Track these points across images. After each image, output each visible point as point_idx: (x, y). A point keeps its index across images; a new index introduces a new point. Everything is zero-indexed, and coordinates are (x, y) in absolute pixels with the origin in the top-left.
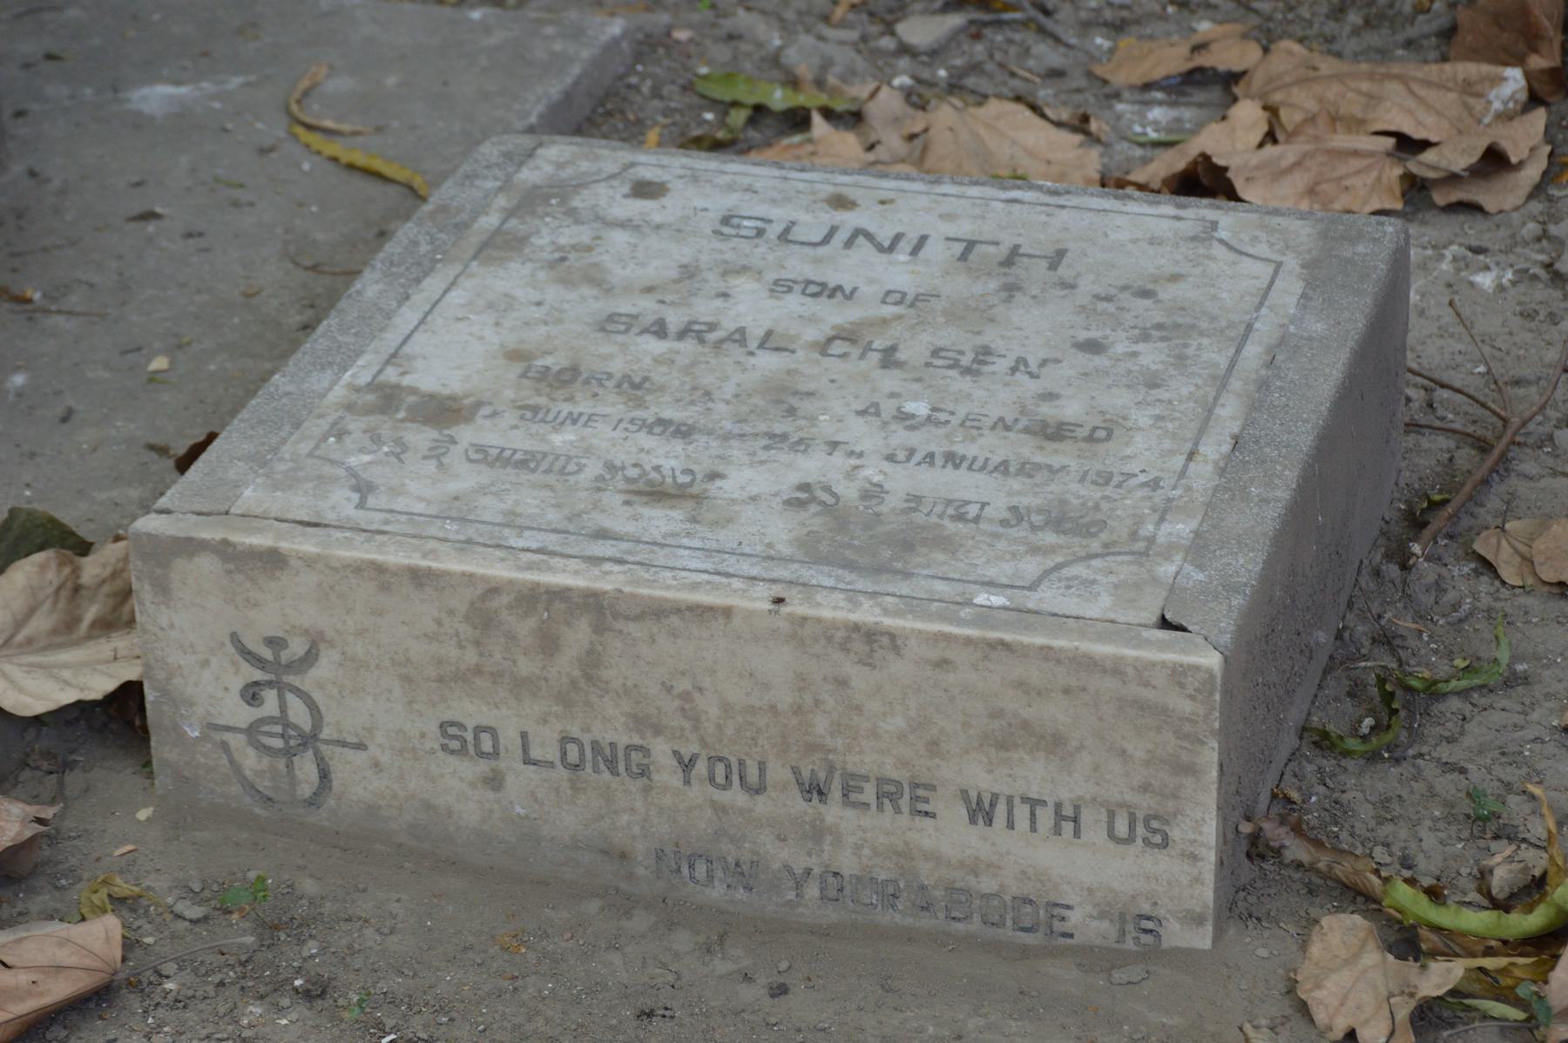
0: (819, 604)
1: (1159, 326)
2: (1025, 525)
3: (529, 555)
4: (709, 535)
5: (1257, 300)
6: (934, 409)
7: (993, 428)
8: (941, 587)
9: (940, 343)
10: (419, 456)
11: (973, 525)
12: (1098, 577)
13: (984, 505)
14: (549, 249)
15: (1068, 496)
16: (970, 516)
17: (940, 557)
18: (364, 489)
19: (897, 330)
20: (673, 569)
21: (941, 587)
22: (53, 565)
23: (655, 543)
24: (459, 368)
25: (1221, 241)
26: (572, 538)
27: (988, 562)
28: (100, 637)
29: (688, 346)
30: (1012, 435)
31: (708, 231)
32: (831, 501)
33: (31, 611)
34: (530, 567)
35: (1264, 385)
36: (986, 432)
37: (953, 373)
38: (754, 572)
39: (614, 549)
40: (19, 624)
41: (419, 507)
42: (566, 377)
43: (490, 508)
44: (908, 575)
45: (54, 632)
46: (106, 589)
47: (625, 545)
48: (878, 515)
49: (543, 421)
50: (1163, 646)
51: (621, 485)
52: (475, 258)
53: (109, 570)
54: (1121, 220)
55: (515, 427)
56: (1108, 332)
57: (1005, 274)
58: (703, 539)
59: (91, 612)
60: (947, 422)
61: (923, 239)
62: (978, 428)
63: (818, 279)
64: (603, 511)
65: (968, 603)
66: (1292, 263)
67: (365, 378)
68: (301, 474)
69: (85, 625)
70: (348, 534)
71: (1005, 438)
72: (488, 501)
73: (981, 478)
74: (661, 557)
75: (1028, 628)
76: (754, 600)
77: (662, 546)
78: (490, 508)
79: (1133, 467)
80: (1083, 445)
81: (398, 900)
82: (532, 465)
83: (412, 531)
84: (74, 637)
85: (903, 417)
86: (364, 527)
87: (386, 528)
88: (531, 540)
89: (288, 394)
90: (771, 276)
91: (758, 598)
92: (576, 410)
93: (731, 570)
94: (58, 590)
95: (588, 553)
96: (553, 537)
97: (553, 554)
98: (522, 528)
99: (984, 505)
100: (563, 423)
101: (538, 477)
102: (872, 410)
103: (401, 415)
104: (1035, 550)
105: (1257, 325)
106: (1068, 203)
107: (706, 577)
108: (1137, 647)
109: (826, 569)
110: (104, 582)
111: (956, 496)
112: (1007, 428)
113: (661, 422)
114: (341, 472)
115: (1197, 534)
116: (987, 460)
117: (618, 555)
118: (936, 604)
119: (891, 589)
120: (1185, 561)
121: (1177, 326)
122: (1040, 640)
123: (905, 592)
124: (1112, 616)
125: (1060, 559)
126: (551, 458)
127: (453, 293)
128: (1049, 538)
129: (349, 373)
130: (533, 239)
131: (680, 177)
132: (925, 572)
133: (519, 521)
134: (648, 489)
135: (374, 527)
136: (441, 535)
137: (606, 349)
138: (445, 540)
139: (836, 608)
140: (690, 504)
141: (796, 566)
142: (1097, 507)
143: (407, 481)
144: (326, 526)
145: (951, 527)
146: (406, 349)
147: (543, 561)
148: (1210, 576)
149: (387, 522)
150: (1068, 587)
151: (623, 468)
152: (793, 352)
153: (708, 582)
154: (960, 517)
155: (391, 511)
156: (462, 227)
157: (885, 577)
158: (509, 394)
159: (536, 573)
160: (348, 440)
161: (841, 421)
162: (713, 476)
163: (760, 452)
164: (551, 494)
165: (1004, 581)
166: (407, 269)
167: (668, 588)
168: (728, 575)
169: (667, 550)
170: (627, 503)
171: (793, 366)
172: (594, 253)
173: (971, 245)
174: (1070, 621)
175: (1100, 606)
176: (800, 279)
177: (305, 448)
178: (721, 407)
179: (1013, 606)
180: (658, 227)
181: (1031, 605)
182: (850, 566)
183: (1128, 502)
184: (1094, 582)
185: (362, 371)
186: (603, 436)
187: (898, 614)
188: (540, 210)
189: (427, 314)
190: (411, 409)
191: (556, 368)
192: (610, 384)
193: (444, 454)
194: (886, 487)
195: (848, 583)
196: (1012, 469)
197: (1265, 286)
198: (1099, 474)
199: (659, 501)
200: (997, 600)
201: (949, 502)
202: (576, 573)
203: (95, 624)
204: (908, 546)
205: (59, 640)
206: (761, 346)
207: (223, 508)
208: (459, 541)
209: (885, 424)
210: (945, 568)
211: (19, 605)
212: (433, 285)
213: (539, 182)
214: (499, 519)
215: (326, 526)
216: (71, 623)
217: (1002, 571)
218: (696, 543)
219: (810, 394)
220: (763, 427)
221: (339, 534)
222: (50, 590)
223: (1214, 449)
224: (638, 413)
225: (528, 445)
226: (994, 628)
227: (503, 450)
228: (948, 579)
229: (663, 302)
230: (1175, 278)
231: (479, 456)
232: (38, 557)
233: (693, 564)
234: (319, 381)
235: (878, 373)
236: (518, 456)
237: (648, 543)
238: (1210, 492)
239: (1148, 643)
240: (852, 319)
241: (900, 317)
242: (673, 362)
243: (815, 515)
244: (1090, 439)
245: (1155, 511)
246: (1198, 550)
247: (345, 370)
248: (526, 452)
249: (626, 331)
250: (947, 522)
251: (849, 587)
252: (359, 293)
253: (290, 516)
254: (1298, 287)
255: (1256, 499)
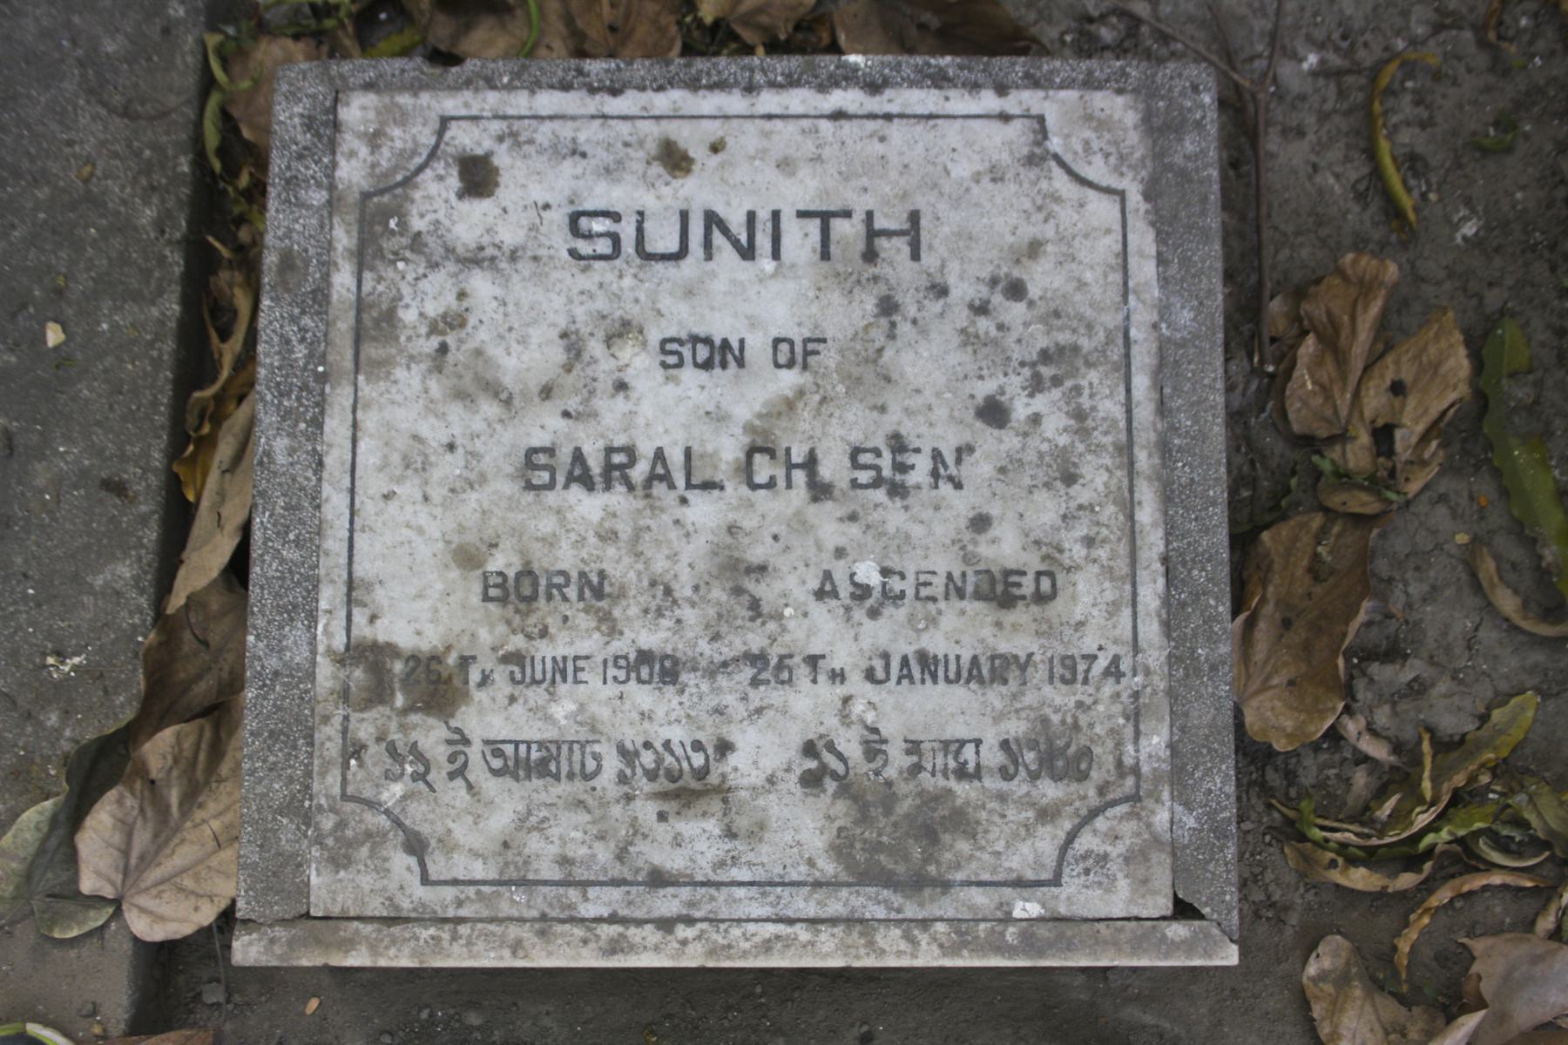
0: (883, 951)
1: (1045, 356)
2: (1023, 773)
3: (605, 926)
4: (751, 856)
5: (1116, 277)
6: (886, 572)
7: (947, 597)
8: (981, 899)
9: (856, 437)
10: (444, 773)
11: (976, 783)
12: (1109, 849)
13: (978, 743)
14: (423, 330)
15: (1047, 711)
16: (971, 767)
17: (964, 846)
18: (416, 846)
19: (805, 420)
20: (739, 921)
21: (981, 899)
22: (127, 794)
23: (707, 884)
24: (420, 596)
25: (1056, 157)
26: (634, 890)
27: (1008, 846)
28: (191, 808)
29: (618, 498)
30: (965, 604)
31: (565, 254)
32: (841, 769)
33: (129, 835)
34: (614, 947)
35: (1164, 448)
36: (942, 605)
37: (880, 495)
38: (811, 911)
39: (676, 902)
40: (126, 853)
41: (479, 871)
42: (527, 591)
43: (542, 855)
44: (946, 886)
45: (156, 836)
46: (175, 773)
47: (685, 892)
48: (889, 784)
49: (535, 682)
50: (1188, 946)
51: (645, 785)
52: (357, 371)
53: (169, 757)
54: (951, 132)
55: (512, 699)
56: (1003, 380)
57: (875, 279)
58: (750, 864)
59: (174, 797)
60: (902, 595)
61: (776, 215)
62: (934, 599)
63: (701, 331)
64: (645, 836)
65: (1008, 919)
66: (1135, 198)
67: (339, 642)
68: (349, 833)
69: (175, 809)
70: (432, 931)
71: (963, 612)
72: (534, 843)
73: (959, 695)
74: (721, 904)
75: (1070, 947)
76: (827, 955)
77: (718, 885)
78: (542, 855)
79: (1089, 644)
80: (1034, 609)
81: (548, 1014)
82: (553, 767)
83: (485, 913)
84: (172, 824)
85: (861, 592)
86: (440, 914)
87: (463, 913)
88: (598, 903)
89: (276, 674)
90: (654, 336)
91: (827, 955)
92: (560, 651)
93: (790, 913)
94: (142, 810)
95: (656, 914)
96: (616, 893)
97: (625, 921)
98: (584, 885)
99: (978, 743)
100: (553, 681)
101: (564, 788)
102: (828, 587)
103: (400, 700)
104: (1047, 814)
105: (1133, 333)
106: (894, 108)
107: (771, 929)
108: (1167, 956)
109: (871, 890)
110: (171, 769)
111: (947, 736)
112: (961, 594)
113: (645, 657)
114: (383, 821)
115: (1171, 746)
116: (958, 657)
117: (684, 912)
118: (982, 926)
119: (939, 913)
120: (1173, 799)
121: (1061, 349)
122: (1084, 963)
123: (950, 914)
124: (1135, 911)
125: (1068, 826)
126: (565, 748)
127: (362, 446)
128: (1050, 790)
129: (320, 627)
130: (401, 313)
131: (501, 139)
132: (960, 876)
133: (580, 873)
134: (672, 786)
135: (451, 913)
136: (516, 914)
137: (547, 525)
138: (521, 920)
139: (899, 953)
140: (716, 805)
141: (844, 893)
142: (1076, 726)
143: (451, 825)
144: (407, 920)
145: (963, 790)
146: (359, 571)
147: (620, 935)
148: (1198, 819)
149: (460, 903)
150: (1087, 872)
151: (637, 754)
152: (722, 488)
153: (778, 937)
154: (962, 773)
155: (455, 882)
156: (321, 296)
157: (927, 892)
158: (485, 636)
159: (620, 956)
160: (367, 757)
161: (805, 615)
162: (724, 748)
163: (752, 693)
164: (588, 818)
165: (1030, 875)
166: (298, 399)
167: (745, 954)
168: (790, 921)
169: (724, 890)
170: (662, 817)
171: (731, 516)
172: (469, 329)
173: (825, 217)
174: (1101, 926)
175: (1119, 901)
176: (684, 335)
177: (333, 780)
178: (689, 614)
179: (1048, 915)
180: (513, 256)
181: (1063, 910)
182: (887, 880)
183: (1101, 708)
184: (1105, 857)
185: (332, 633)
186: (596, 691)
187: (953, 950)
188: (388, 245)
189: (352, 491)
190: (408, 682)
191: (511, 574)
192: (572, 592)
193: (465, 764)
194: (884, 732)
195: (899, 911)
196: (985, 672)
197: (1119, 247)
198: (1064, 658)
199: (688, 805)
200: (1034, 910)
201: (946, 744)
202: (657, 949)
203: (181, 804)
204: (930, 834)
205: (163, 837)
206: (689, 486)
207: (303, 911)
208: (533, 920)
209: (848, 609)
210: (974, 865)
211: (117, 839)
212: (336, 427)
213: (366, 185)
214: (556, 874)
215: (407, 920)
216: (163, 810)
217: (1019, 860)
218: (744, 875)
219: (762, 569)
220: (739, 648)
221: (426, 933)
222: (135, 812)
223: (1151, 592)
224: (618, 646)
225: (533, 731)
226: (1041, 954)
227: (517, 744)
228: (980, 884)
229: (566, 414)
230: (1034, 249)
231: (497, 763)
232: (112, 795)
233: (757, 911)
234: (295, 635)
235: (813, 509)
236: (535, 755)
237: (703, 884)
238: (1166, 669)
239: (1174, 947)
240: (757, 408)
241: (801, 393)
242: (616, 534)
243: (836, 796)
244: (1040, 598)
245: (1127, 719)
246: (1179, 773)
247: (312, 618)
248: (541, 744)
249: (551, 486)
250: (952, 783)
251: (900, 916)
252: (268, 454)
253: (369, 913)
254: (1150, 235)
255: (1206, 667)
